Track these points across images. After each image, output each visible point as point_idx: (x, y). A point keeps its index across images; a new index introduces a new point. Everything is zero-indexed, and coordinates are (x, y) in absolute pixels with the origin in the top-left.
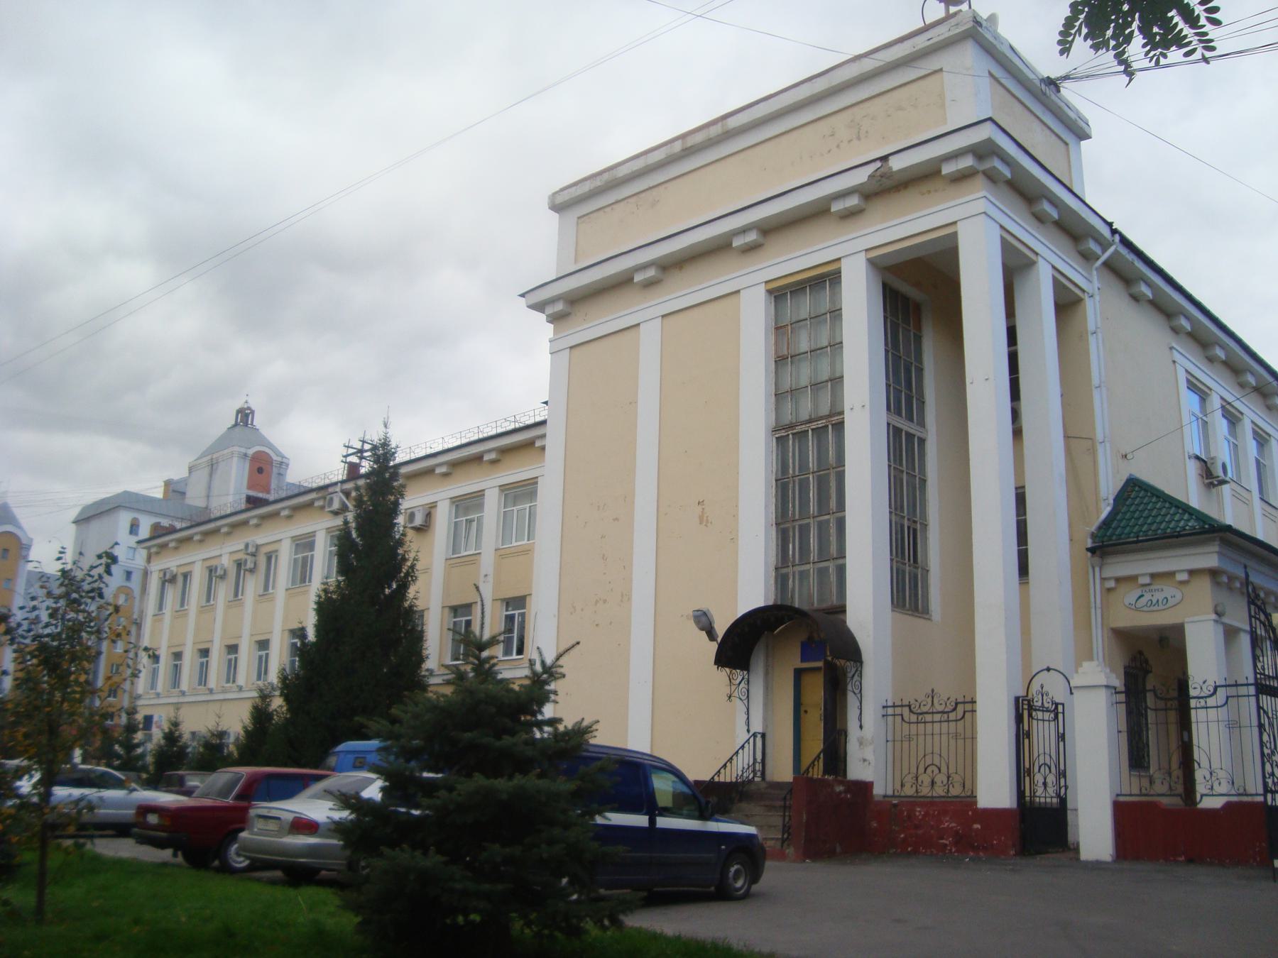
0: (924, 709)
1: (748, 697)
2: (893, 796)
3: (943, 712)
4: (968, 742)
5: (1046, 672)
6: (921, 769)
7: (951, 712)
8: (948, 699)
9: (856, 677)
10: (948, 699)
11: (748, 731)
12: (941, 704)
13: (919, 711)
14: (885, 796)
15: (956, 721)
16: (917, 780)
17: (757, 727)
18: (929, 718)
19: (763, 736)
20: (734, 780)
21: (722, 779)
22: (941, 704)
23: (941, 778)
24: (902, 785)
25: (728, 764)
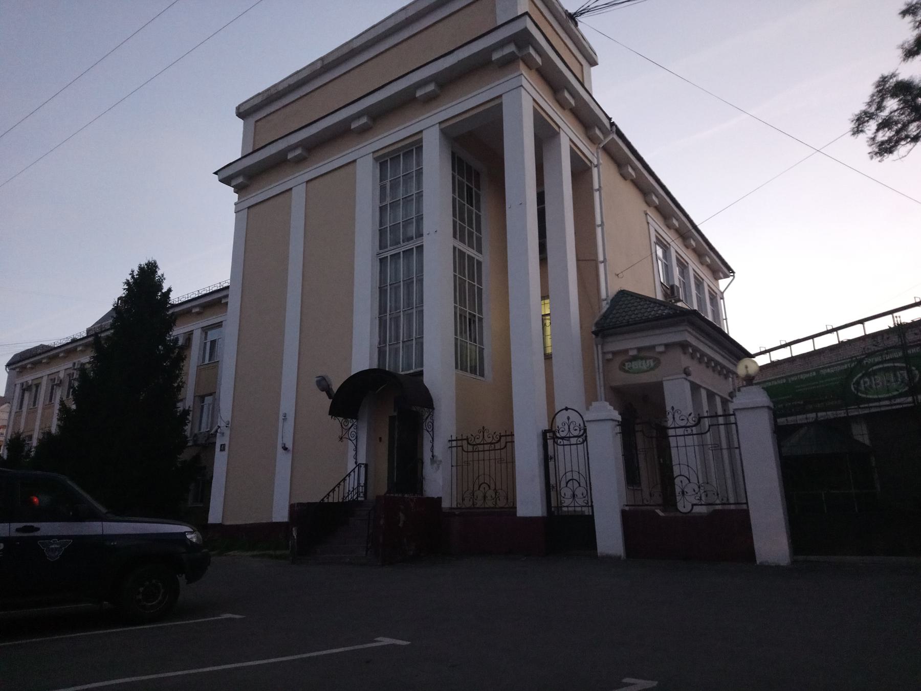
0: (478, 441)
1: (356, 438)
2: (457, 508)
3: (491, 443)
4: (510, 465)
5: (564, 411)
6: (476, 487)
7: (497, 443)
8: (495, 433)
9: (429, 420)
10: (495, 433)
11: (356, 463)
12: (682, 420)
13: (475, 443)
14: (451, 508)
15: (501, 449)
16: (473, 495)
17: (362, 459)
18: (481, 448)
19: (366, 466)
20: (341, 501)
21: (331, 500)
22: (682, 420)
23: (490, 493)
24: (463, 500)
25: (337, 489)
